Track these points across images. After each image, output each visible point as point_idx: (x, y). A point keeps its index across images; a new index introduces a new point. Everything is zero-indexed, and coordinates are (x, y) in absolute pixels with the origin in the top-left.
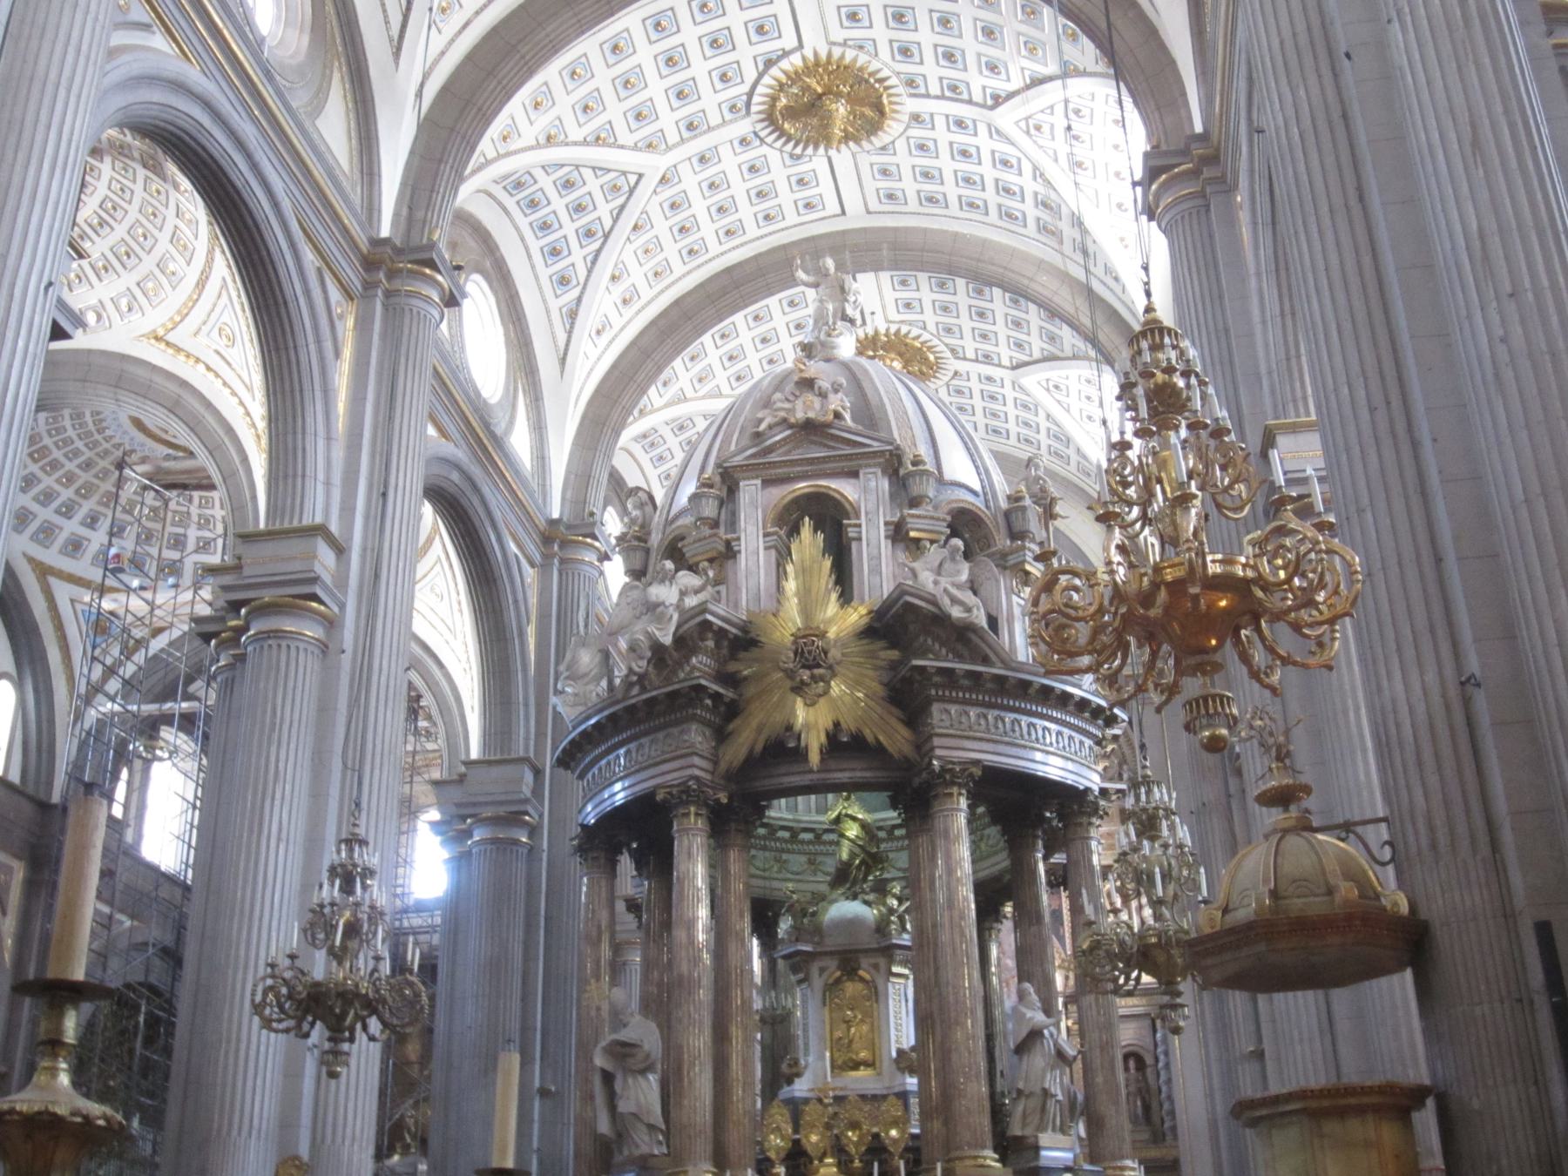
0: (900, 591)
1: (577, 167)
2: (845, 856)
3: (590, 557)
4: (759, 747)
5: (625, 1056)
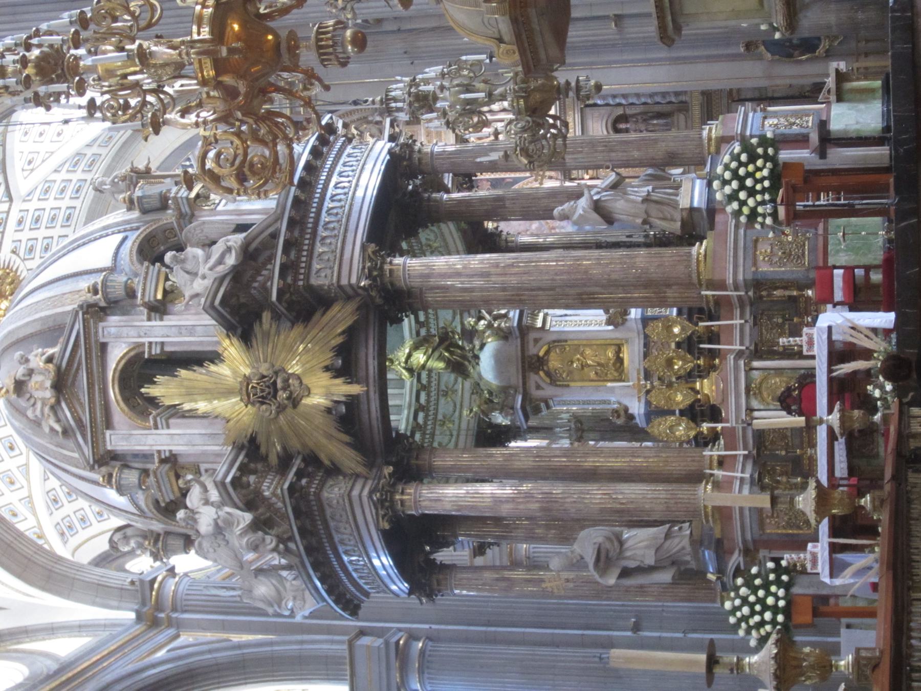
0: (210, 308)
2: (441, 365)
3: (171, 585)
4: (347, 438)
5: (607, 557)
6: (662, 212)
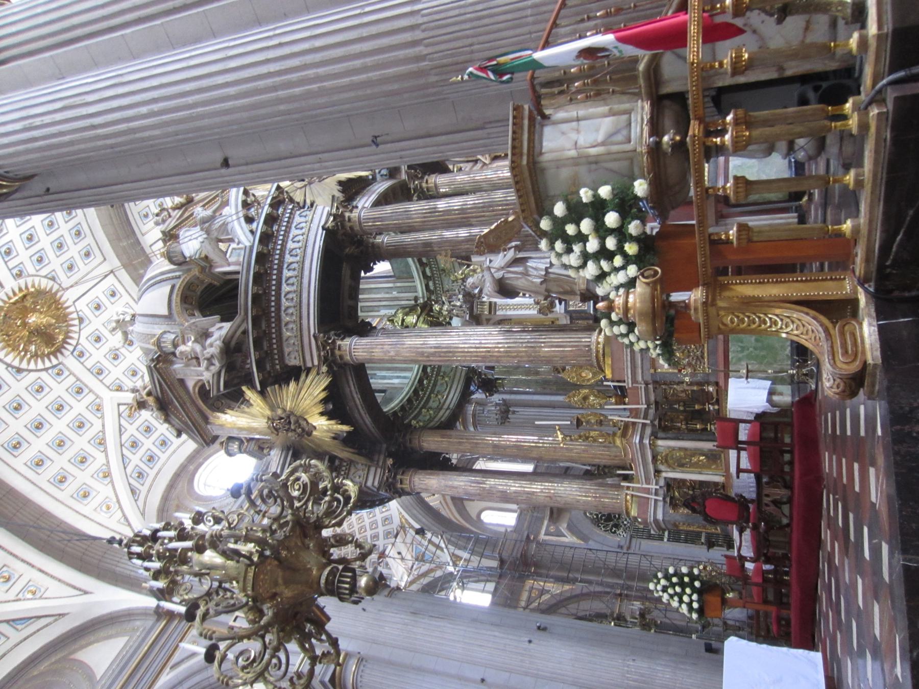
1: (121, 446)
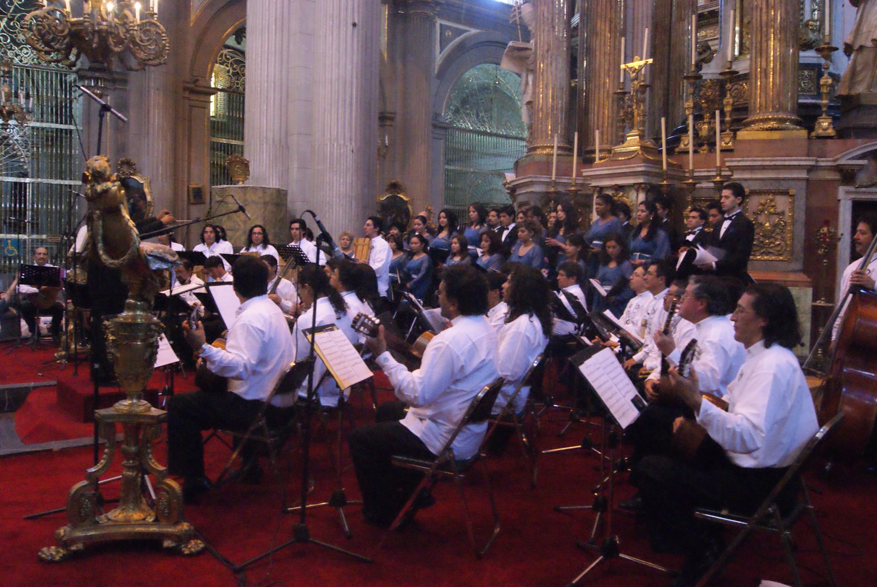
6: (863, 69)
